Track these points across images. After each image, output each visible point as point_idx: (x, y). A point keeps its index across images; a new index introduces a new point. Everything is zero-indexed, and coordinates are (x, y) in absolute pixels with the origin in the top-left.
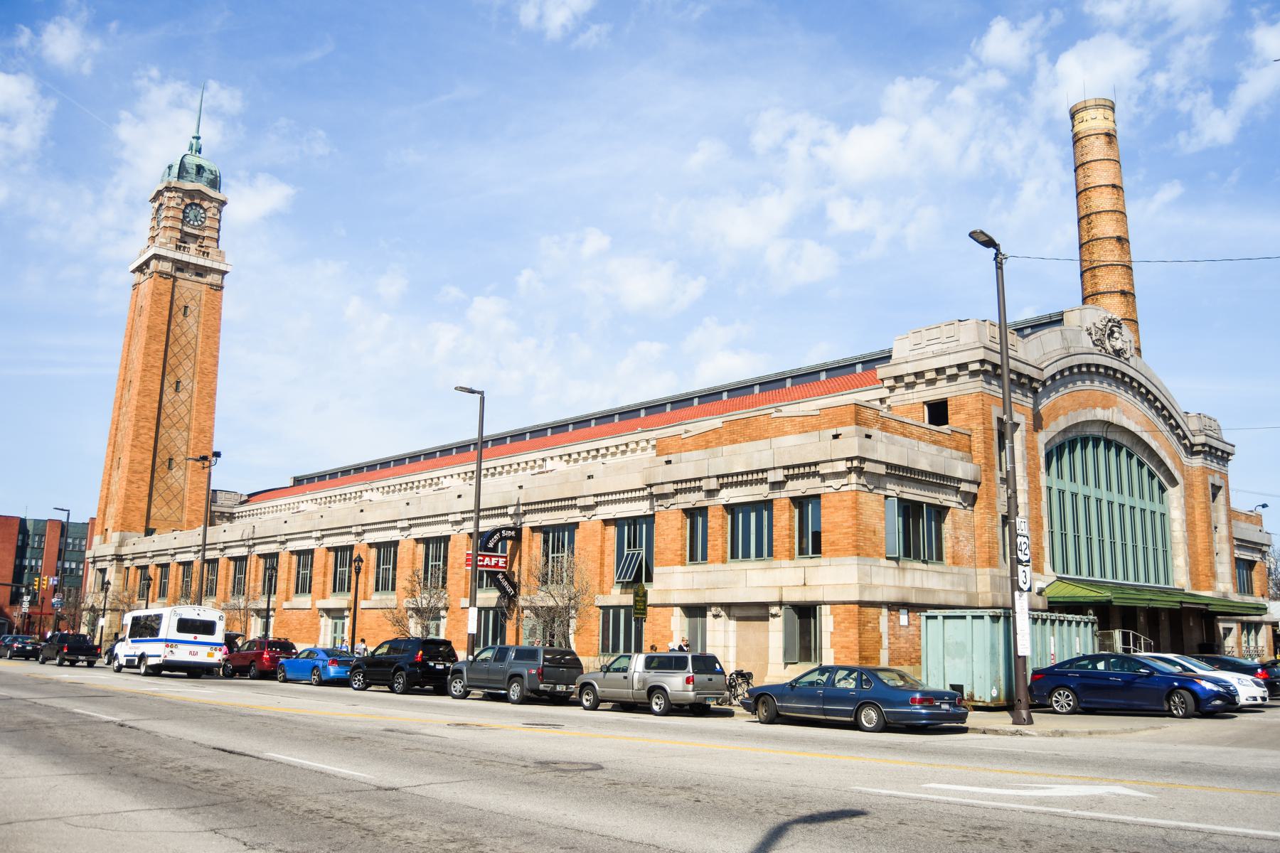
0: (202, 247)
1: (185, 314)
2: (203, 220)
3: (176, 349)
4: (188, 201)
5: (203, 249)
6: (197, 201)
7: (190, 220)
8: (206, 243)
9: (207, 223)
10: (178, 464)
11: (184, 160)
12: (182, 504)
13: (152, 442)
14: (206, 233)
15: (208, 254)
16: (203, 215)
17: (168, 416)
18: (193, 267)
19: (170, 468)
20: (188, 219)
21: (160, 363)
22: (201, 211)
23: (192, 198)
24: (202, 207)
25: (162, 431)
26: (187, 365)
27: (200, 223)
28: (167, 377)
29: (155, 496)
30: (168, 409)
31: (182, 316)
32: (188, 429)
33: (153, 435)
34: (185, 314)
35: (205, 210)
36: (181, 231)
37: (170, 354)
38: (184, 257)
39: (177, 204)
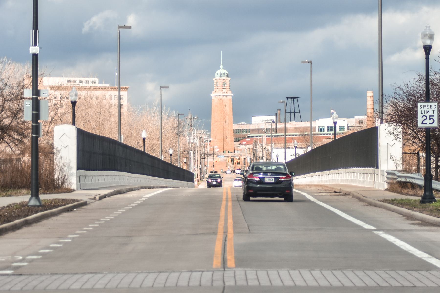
1: (225, 106)
3: (225, 114)
9: (227, 85)
10: (228, 137)
11: (221, 72)
12: (229, 145)
13: (223, 134)
17: (225, 128)
19: (226, 139)
21: (222, 118)
25: (224, 131)
26: (227, 117)
28: (224, 120)
29: (224, 144)
30: (225, 127)
31: (225, 107)
32: (228, 130)
33: (223, 132)
34: (225, 106)
37: (224, 115)
38: (224, 95)
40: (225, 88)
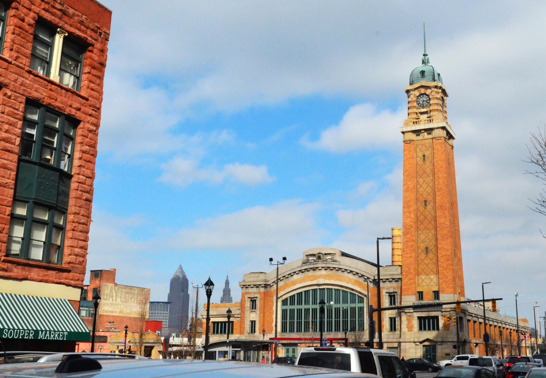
2: (428, 101)
4: (418, 94)
9: (431, 102)
14: (431, 108)
18: (424, 131)
20: (420, 105)
22: (427, 97)
24: (427, 95)
27: (427, 104)
35: (428, 96)
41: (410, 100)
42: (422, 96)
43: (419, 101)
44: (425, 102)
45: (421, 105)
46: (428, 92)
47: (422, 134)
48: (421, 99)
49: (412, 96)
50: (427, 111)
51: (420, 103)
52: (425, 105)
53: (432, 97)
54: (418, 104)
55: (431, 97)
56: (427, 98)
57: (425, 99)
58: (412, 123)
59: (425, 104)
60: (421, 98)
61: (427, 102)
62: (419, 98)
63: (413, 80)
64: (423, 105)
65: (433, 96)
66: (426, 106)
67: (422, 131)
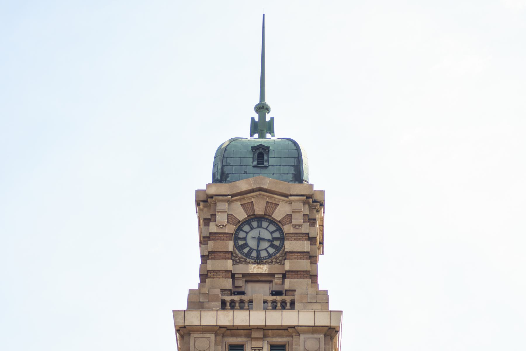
0: (278, 293)
2: (277, 243)
4: (241, 215)
5: (279, 298)
6: (259, 209)
7: (251, 250)
8: (288, 284)
9: (288, 246)
14: (288, 265)
15: (292, 304)
16: (277, 235)
18: (259, 334)
20: (246, 250)
22: (272, 228)
23: (248, 206)
24: (272, 222)
27: (271, 250)
35: (278, 225)
36: (233, 276)
39: (218, 226)
40: (264, 269)
41: (213, 228)
42: (255, 224)
43: (245, 239)
44: (264, 245)
45: (251, 250)
46: (278, 214)
47: (255, 344)
48: (255, 233)
49: (222, 218)
50: (273, 275)
51: (246, 245)
52: (264, 254)
53: (292, 230)
54: (241, 248)
55: (287, 229)
56: (272, 233)
57: (266, 235)
58: (219, 304)
59: (266, 249)
60: (252, 228)
61: (272, 246)
62: (246, 228)
63: (226, 170)
64: (258, 252)
65: (295, 227)
66: (270, 256)
67: (254, 334)
